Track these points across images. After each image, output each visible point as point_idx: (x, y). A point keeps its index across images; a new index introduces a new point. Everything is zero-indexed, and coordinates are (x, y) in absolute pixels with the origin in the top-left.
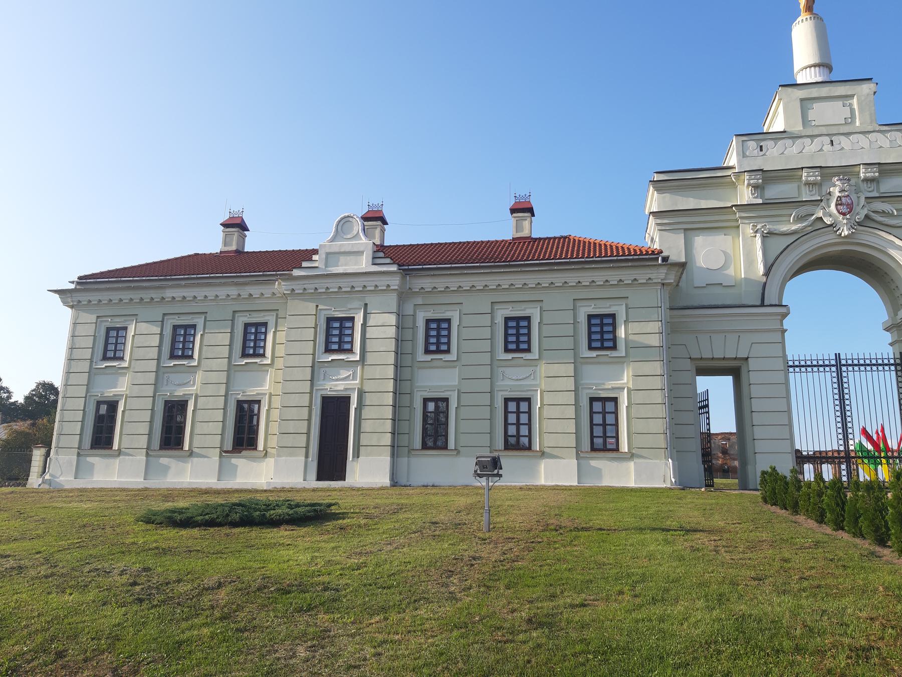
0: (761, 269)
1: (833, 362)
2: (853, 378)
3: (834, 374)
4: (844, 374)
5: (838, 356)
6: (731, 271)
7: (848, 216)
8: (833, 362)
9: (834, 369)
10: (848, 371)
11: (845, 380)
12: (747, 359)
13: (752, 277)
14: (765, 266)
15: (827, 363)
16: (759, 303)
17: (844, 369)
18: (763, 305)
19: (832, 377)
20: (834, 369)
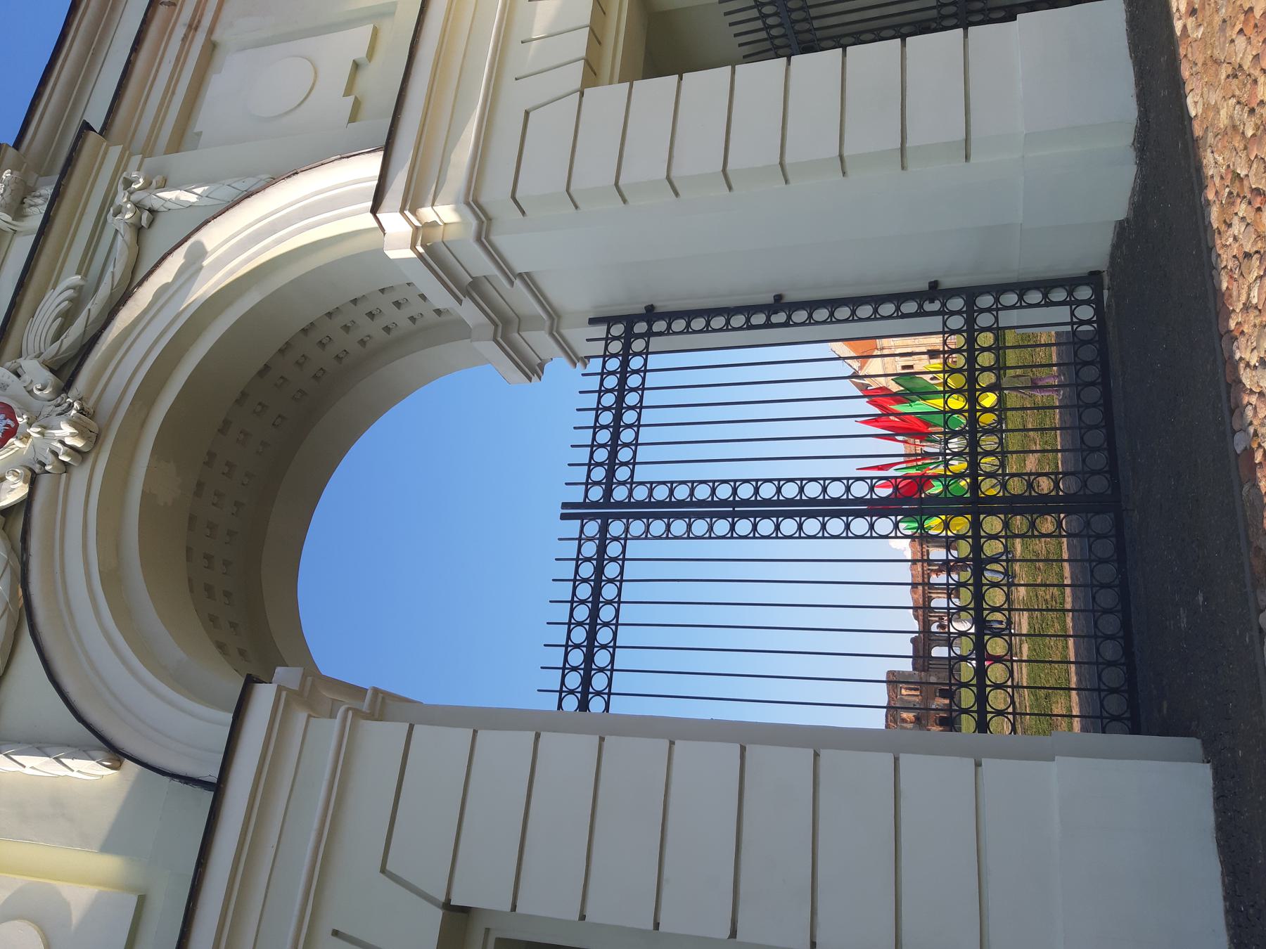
0: (89, 772)
1: (592, 528)
2: (660, 464)
3: (637, 527)
4: (640, 494)
5: (571, 511)
6: (79, 897)
7: (22, 420)
8: (592, 528)
9: (616, 528)
10: (631, 483)
11: (661, 493)
12: (447, 906)
13: (107, 814)
14: (81, 751)
15: (590, 549)
16: (208, 796)
17: (620, 494)
18: (218, 788)
19: (646, 535)
20: (616, 528)
